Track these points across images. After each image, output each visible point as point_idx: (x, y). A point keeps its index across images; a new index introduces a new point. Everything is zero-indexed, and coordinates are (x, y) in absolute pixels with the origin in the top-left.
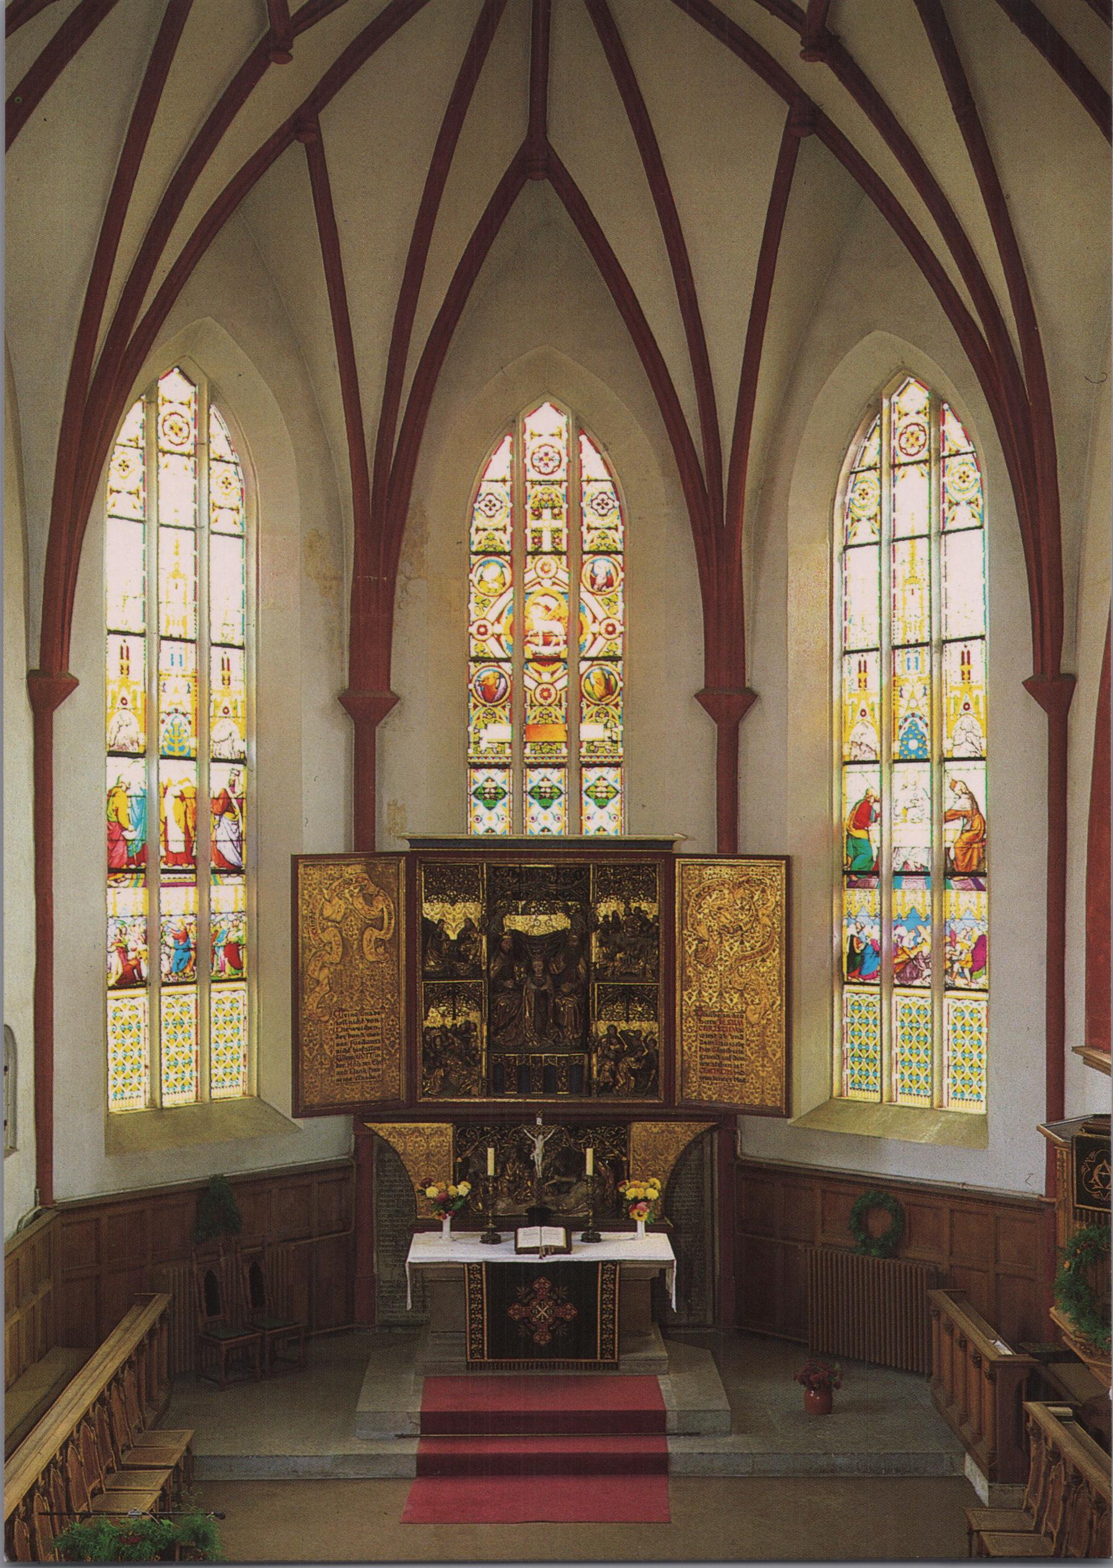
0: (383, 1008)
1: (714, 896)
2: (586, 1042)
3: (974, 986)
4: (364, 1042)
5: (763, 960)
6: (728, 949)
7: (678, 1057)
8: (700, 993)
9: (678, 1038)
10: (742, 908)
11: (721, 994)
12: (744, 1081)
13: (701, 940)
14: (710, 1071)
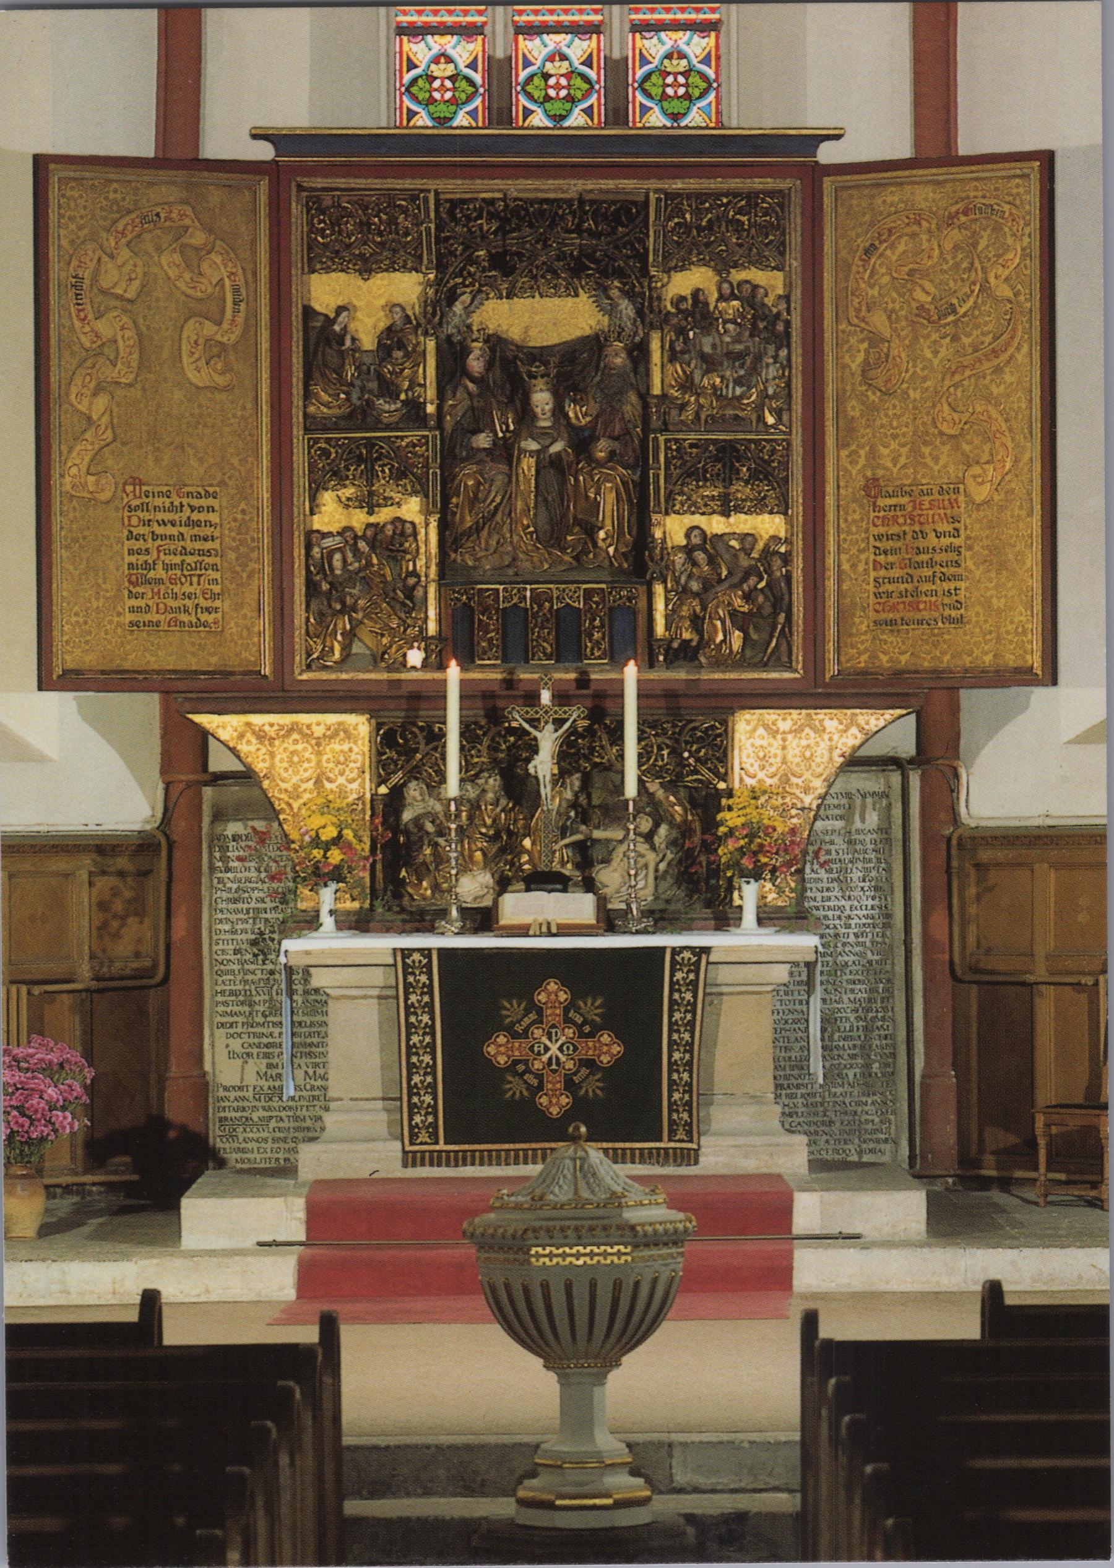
1: (901, 248)
4: (184, 552)
5: (998, 370)
6: (928, 354)
7: (831, 584)
9: (831, 546)
12: (960, 620)
14: (893, 608)
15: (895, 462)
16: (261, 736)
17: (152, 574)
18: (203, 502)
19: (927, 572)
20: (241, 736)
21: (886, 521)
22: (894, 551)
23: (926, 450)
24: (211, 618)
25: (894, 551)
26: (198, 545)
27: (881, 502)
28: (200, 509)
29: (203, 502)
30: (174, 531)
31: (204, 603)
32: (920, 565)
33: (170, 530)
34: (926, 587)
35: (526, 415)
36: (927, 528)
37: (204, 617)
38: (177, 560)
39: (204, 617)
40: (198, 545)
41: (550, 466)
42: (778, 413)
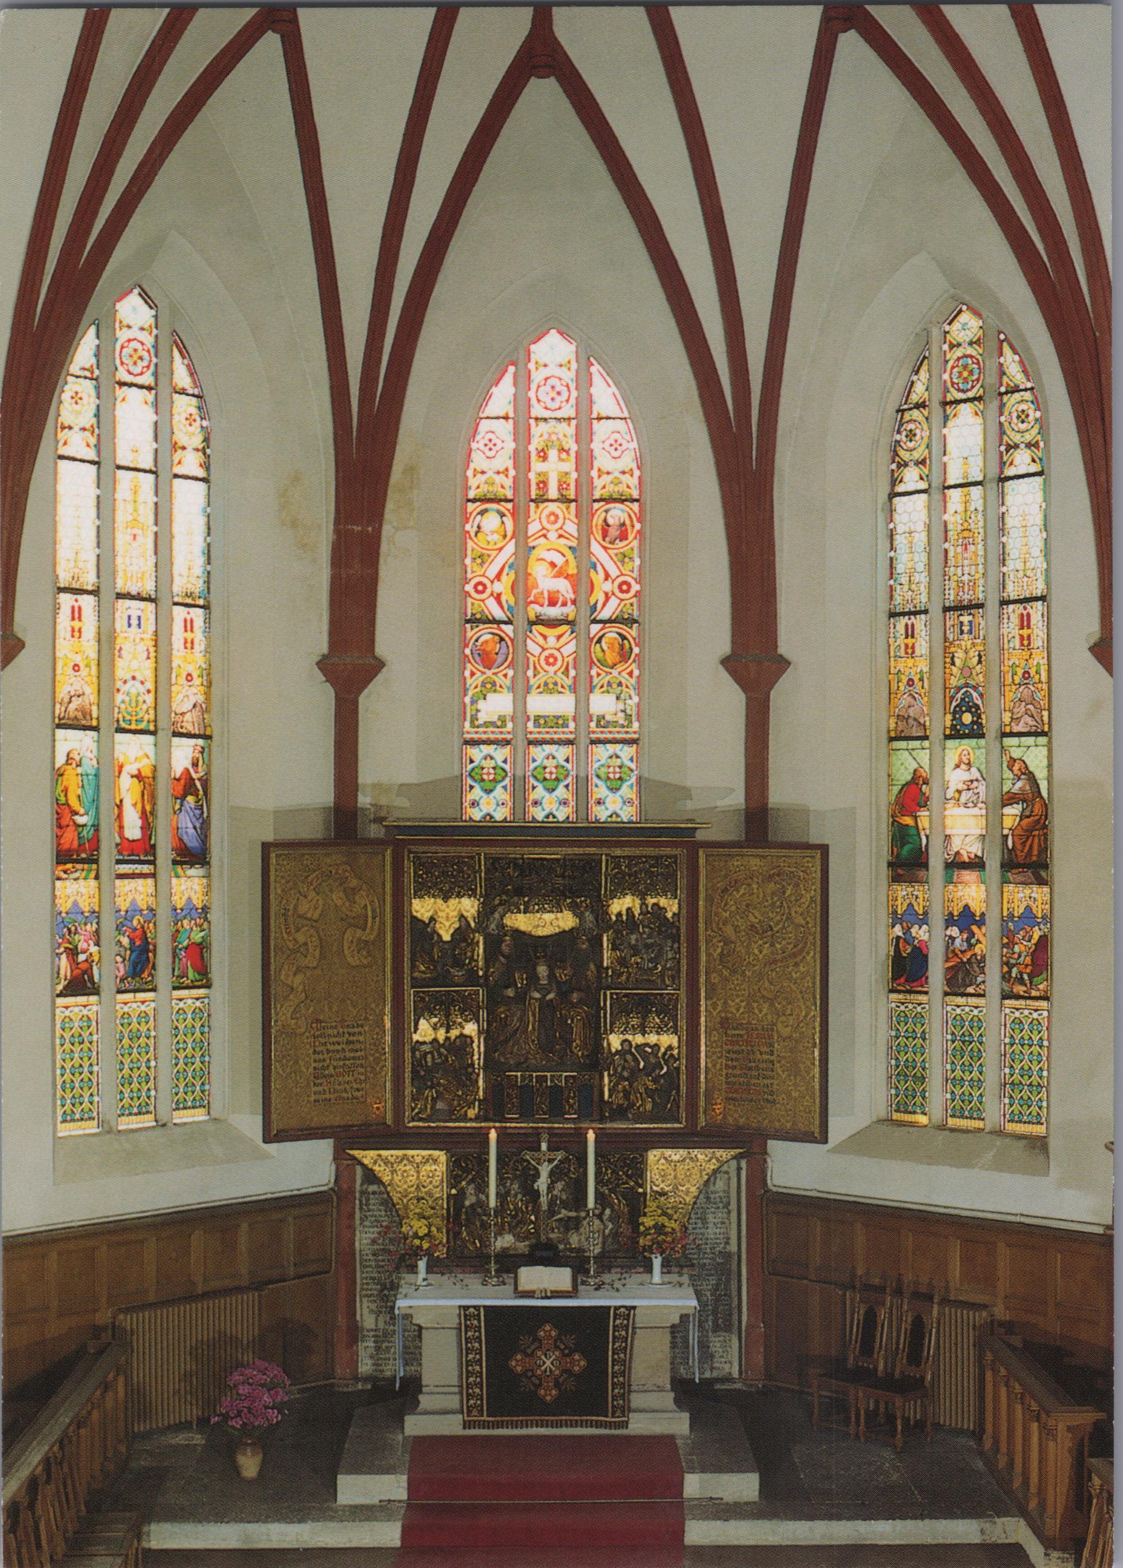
0: (366, 1018)
1: (742, 891)
3: (1034, 993)
4: (345, 1059)
8: (725, 1003)
10: (773, 904)
11: (748, 1004)
13: (727, 942)
14: (736, 1091)
16: (386, 1162)
18: (356, 1030)
19: (754, 1073)
20: (375, 1162)
21: (732, 1043)
22: (737, 1060)
24: (359, 1094)
25: (737, 1060)
26: (352, 1055)
27: (729, 1032)
28: (354, 1034)
29: (356, 1030)
30: (339, 1048)
31: (355, 1086)
32: (750, 1069)
36: (755, 1049)
37: (356, 1094)
38: (341, 1063)
39: (356, 1094)
40: (352, 1055)
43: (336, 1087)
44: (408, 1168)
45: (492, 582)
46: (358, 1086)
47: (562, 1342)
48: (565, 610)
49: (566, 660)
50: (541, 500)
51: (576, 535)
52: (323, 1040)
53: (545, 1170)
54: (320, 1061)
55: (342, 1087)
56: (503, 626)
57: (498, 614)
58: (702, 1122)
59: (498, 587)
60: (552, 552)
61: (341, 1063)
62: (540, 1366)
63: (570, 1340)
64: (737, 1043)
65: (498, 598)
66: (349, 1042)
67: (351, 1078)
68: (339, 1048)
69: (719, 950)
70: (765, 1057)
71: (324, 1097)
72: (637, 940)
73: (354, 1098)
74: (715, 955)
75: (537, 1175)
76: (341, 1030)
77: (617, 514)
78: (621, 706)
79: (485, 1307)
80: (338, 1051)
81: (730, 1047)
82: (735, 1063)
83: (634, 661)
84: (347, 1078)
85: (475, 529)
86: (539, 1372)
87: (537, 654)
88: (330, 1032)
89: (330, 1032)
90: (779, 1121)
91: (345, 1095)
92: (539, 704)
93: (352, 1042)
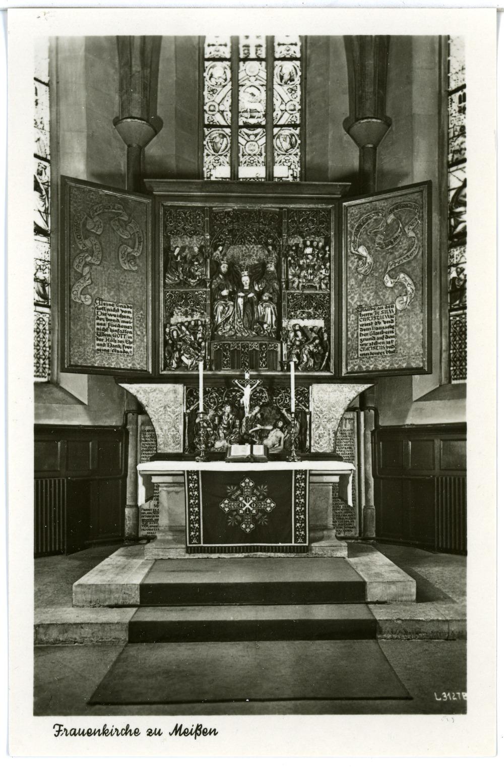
2: (279, 333)
4: (119, 326)
14: (368, 349)
15: (368, 298)
17: (106, 333)
20: (138, 391)
21: (365, 320)
22: (368, 329)
23: (380, 293)
25: (368, 329)
28: (125, 312)
30: (115, 318)
31: (126, 345)
32: (378, 333)
33: (113, 318)
34: (379, 341)
35: (240, 285)
36: (381, 321)
37: (126, 350)
38: (116, 328)
39: (126, 350)
41: (248, 302)
42: (326, 285)
43: (113, 343)
44: (159, 396)
45: (219, 104)
46: (128, 345)
47: (258, 490)
48: (260, 120)
49: (260, 147)
50: (246, 59)
51: (265, 78)
52: (104, 312)
53: (248, 391)
54: (101, 324)
55: (117, 344)
56: (224, 129)
57: (223, 123)
58: (344, 371)
59: (222, 108)
60: (252, 88)
61: (116, 328)
62: (242, 507)
63: (264, 521)
64: (368, 319)
65: (222, 112)
66: (121, 316)
67: (123, 339)
68: (115, 318)
69: (355, 264)
70: (387, 325)
71: (104, 348)
72: (304, 263)
73: (124, 352)
74: (353, 268)
75: (242, 395)
76: (116, 308)
77: (288, 67)
78: (291, 172)
79: (204, 472)
80: (114, 321)
81: (363, 322)
82: (366, 332)
83: (298, 148)
84: (120, 339)
85: (209, 75)
86: (241, 512)
87: (244, 144)
88: (109, 307)
89: (109, 307)
90: (397, 364)
91: (118, 349)
92: (245, 172)
93: (124, 317)
